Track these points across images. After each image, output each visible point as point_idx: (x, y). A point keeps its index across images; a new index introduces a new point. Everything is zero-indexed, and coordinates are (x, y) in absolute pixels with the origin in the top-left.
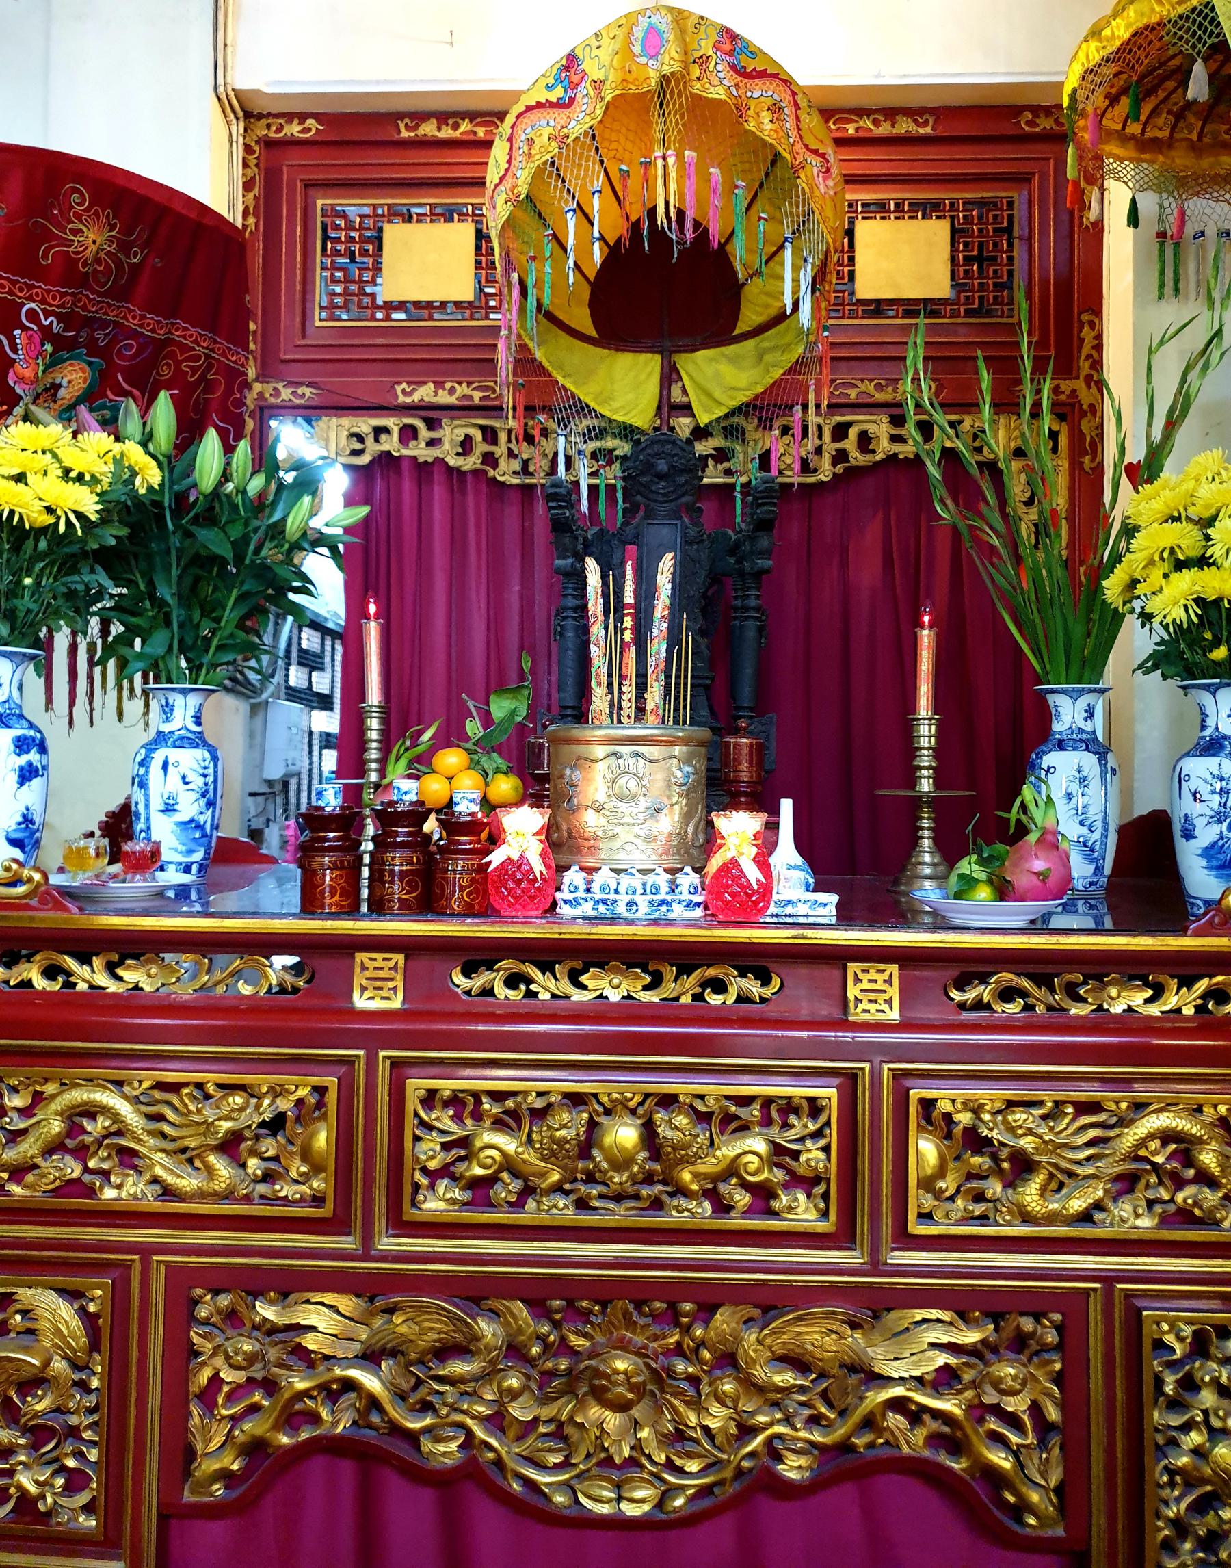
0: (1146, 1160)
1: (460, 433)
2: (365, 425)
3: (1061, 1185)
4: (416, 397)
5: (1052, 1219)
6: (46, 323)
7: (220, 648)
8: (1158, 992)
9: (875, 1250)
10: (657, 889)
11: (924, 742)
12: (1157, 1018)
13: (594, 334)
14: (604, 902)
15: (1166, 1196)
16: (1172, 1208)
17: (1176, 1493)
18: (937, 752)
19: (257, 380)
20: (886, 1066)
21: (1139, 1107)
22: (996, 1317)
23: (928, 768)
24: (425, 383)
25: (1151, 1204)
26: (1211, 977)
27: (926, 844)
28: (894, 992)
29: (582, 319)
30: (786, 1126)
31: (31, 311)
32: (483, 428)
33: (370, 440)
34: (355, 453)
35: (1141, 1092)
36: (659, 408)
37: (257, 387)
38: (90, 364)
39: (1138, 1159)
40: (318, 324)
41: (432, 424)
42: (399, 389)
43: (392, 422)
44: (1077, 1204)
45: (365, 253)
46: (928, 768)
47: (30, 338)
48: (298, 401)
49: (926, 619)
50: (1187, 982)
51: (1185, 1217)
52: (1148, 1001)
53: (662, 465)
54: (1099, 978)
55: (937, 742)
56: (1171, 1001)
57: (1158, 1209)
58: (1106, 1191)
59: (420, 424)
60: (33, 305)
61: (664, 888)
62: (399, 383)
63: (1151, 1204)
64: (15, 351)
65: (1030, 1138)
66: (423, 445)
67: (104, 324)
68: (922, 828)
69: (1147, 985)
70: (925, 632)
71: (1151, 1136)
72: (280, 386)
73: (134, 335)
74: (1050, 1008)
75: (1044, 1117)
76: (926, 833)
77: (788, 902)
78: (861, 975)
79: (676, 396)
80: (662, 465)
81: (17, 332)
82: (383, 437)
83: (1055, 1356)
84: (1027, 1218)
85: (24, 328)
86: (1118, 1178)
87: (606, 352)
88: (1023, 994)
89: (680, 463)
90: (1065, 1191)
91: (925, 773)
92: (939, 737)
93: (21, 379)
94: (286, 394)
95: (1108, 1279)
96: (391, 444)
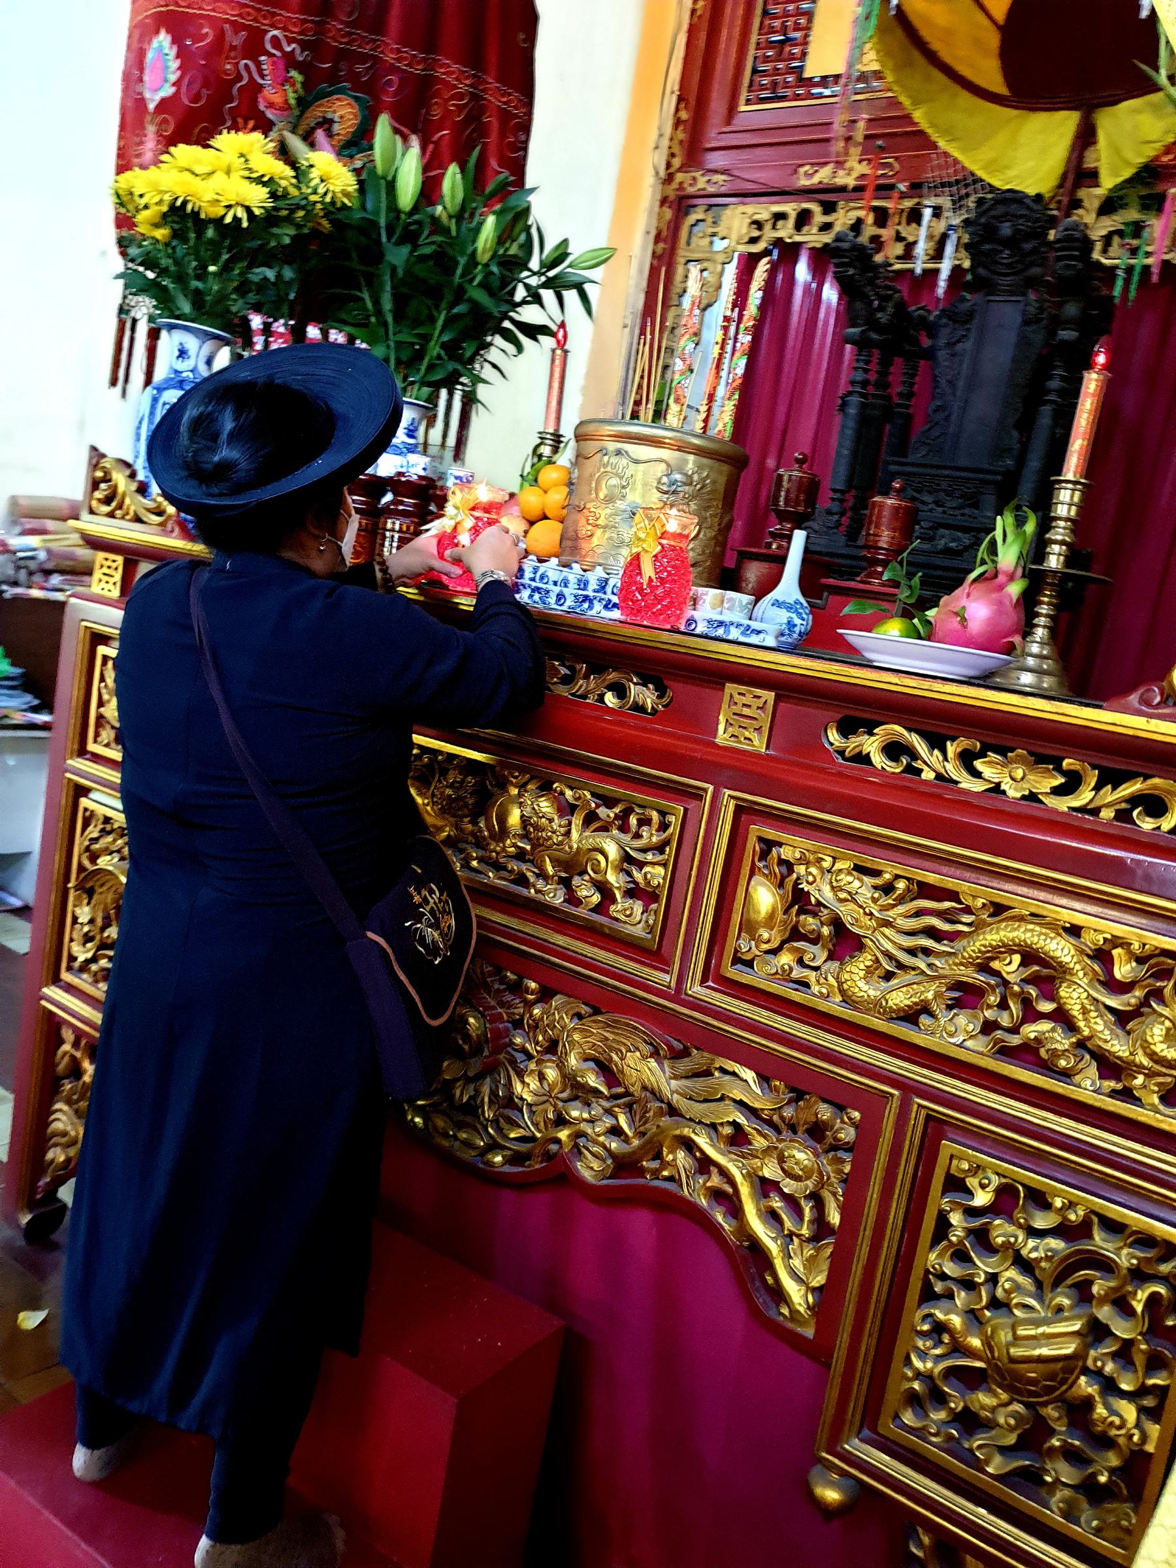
0: (997, 974)
1: (854, 215)
2: (763, 210)
3: (888, 976)
4: (816, 180)
5: (876, 1006)
6: (288, 49)
7: (431, 367)
8: (1071, 785)
9: (680, 980)
10: (586, 584)
11: (1062, 511)
12: (1063, 813)
13: (1003, 90)
14: (538, 589)
15: (1005, 1020)
16: (1015, 1040)
17: (938, 1351)
18: (1077, 525)
19: (679, 170)
20: (711, 788)
21: (998, 909)
22: (798, 1095)
23: (1062, 543)
24: (826, 163)
25: (989, 1027)
26: (1147, 777)
27: (1040, 633)
28: (765, 720)
29: (991, 76)
30: (637, 836)
31: (274, 38)
32: (875, 209)
33: (768, 227)
34: (753, 241)
35: (1007, 892)
36: (1064, 176)
37: (679, 177)
38: (356, 99)
39: (984, 968)
40: (743, 108)
41: (829, 208)
42: (802, 170)
43: (791, 208)
44: (899, 999)
45: (797, 28)
46: (1062, 543)
47: (274, 63)
48: (711, 189)
49: (1101, 359)
50: (1110, 778)
51: (1028, 1054)
52: (1057, 791)
53: (1006, 229)
54: (1002, 751)
55: (1078, 514)
56: (1084, 796)
57: (999, 1034)
58: (937, 995)
59: (815, 208)
60: (276, 32)
61: (593, 585)
62: (802, 165)
63: (989, 1027)
64: (262, 76)
65: (852, 906)
66: (815, 230)
67: (363, 58)
68: (1038, 615)
69: (1059, 769)
70: (1094, 376)
71: (1009, 949)
72: (697, 174)
73: (393, 69)
74: (939, 776)
75: (875, 888)
76: (1042, 621)
77: (721, 623)
78: (737, 697)
79: (1089, 164)
80: (1006, 229)
81: (263, 58)
82: (780, 223)
83: (848, 1157)
84: (848, 999)
85: (270, 55)
86: (959, 986)
87: (1015, 112)
88: (914, 756)
89: (1023, 224)
90: (894, 982)
91: (1056, 548)
92: (1083, 507)
93: (271, 105)
94: (702, 183)
95: (909, 1088)
96: (786, 232)
